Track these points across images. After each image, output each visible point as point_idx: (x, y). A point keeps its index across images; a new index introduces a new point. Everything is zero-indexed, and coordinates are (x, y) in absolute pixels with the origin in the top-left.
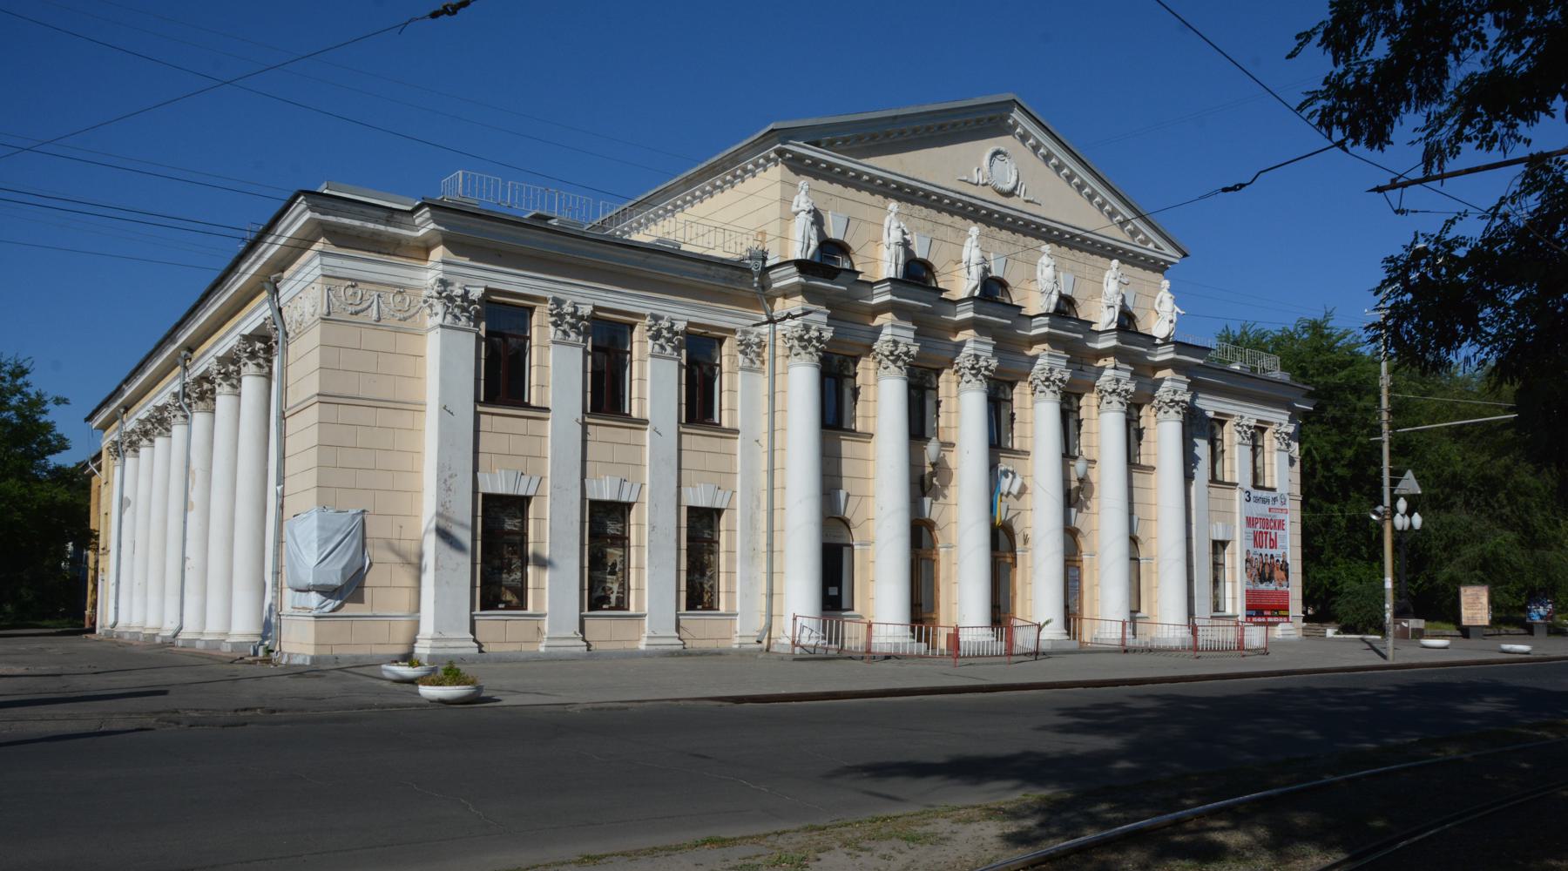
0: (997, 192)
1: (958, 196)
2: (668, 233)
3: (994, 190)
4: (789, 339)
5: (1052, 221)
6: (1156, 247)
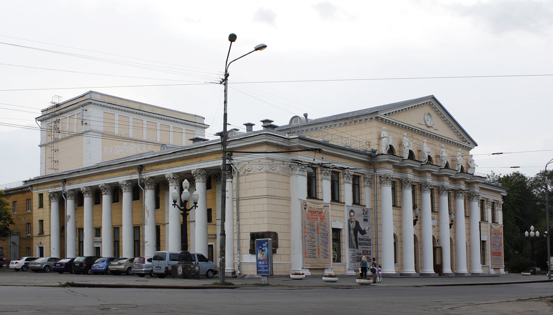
1: (420, 129)
2: (347, 143)
4: (382, 178)
5: (443, 136)
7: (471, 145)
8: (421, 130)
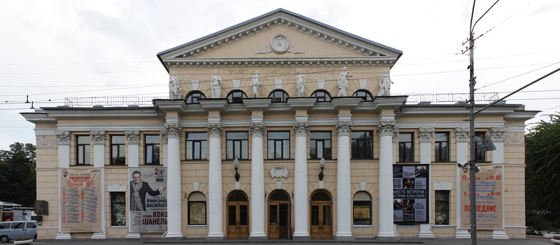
0: (278, 53)
3: (276, 53)
6: (380, 55)
7: (388, 55)
8: (254, 60)
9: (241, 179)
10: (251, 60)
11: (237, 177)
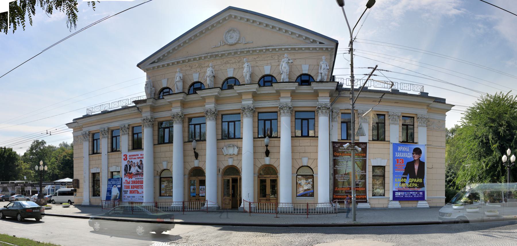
9: (199, 157)
10: (206, 55)
11: (197, 156)
